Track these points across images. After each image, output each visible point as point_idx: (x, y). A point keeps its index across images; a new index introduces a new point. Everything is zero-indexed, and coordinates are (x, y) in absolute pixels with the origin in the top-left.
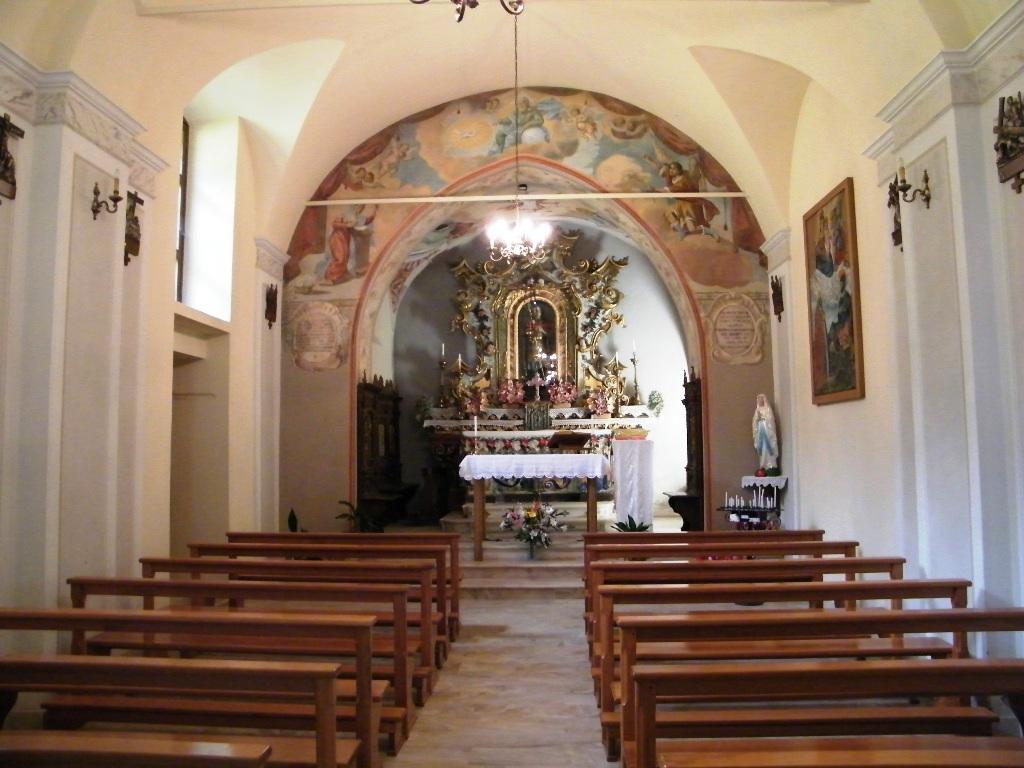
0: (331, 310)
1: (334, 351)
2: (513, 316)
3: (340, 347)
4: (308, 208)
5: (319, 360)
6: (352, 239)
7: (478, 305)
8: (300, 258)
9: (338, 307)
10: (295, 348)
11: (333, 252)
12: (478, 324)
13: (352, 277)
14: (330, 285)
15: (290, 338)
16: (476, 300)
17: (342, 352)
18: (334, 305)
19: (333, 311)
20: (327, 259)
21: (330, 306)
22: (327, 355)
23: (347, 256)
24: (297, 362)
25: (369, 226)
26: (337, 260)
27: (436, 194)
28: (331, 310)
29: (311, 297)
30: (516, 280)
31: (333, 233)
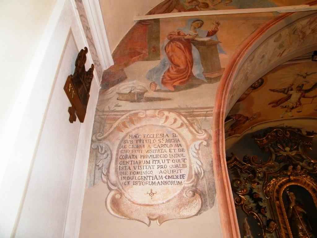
0: (175, 121)
1: (186, 183)
2: (278, 199)
3: (197, 175)
4: (140, 22)
5: (159, 199)
6: (194, 48)
7: (252, 189)
8: (126, 65)
9: (185, 117)
10: (113, 177)
11: (170, 59)
12: (254, 205)
13: (200, 83)
14: (170, 91)
15: (103, 163)
16: (248, 185)
17: (203, 185)
18: (180, 114)
19: (179, 122)
20: (164, 65)
21: (173, 115)
22: (174, 190)
23: (190, 63)
24: (115, 203)
25: (213, 38)
26: (177, 66)
27: (296, 13)
28: (175, 121)
29: (143, 105)
30: (277, 169)
31: (169, 43)
